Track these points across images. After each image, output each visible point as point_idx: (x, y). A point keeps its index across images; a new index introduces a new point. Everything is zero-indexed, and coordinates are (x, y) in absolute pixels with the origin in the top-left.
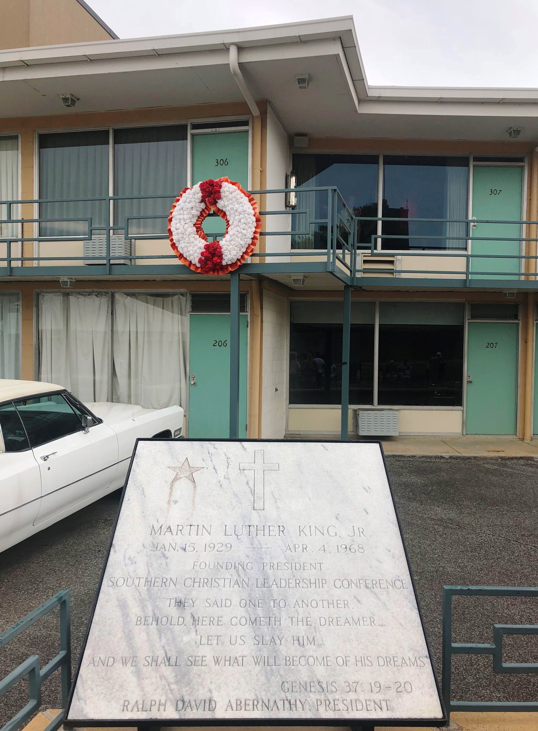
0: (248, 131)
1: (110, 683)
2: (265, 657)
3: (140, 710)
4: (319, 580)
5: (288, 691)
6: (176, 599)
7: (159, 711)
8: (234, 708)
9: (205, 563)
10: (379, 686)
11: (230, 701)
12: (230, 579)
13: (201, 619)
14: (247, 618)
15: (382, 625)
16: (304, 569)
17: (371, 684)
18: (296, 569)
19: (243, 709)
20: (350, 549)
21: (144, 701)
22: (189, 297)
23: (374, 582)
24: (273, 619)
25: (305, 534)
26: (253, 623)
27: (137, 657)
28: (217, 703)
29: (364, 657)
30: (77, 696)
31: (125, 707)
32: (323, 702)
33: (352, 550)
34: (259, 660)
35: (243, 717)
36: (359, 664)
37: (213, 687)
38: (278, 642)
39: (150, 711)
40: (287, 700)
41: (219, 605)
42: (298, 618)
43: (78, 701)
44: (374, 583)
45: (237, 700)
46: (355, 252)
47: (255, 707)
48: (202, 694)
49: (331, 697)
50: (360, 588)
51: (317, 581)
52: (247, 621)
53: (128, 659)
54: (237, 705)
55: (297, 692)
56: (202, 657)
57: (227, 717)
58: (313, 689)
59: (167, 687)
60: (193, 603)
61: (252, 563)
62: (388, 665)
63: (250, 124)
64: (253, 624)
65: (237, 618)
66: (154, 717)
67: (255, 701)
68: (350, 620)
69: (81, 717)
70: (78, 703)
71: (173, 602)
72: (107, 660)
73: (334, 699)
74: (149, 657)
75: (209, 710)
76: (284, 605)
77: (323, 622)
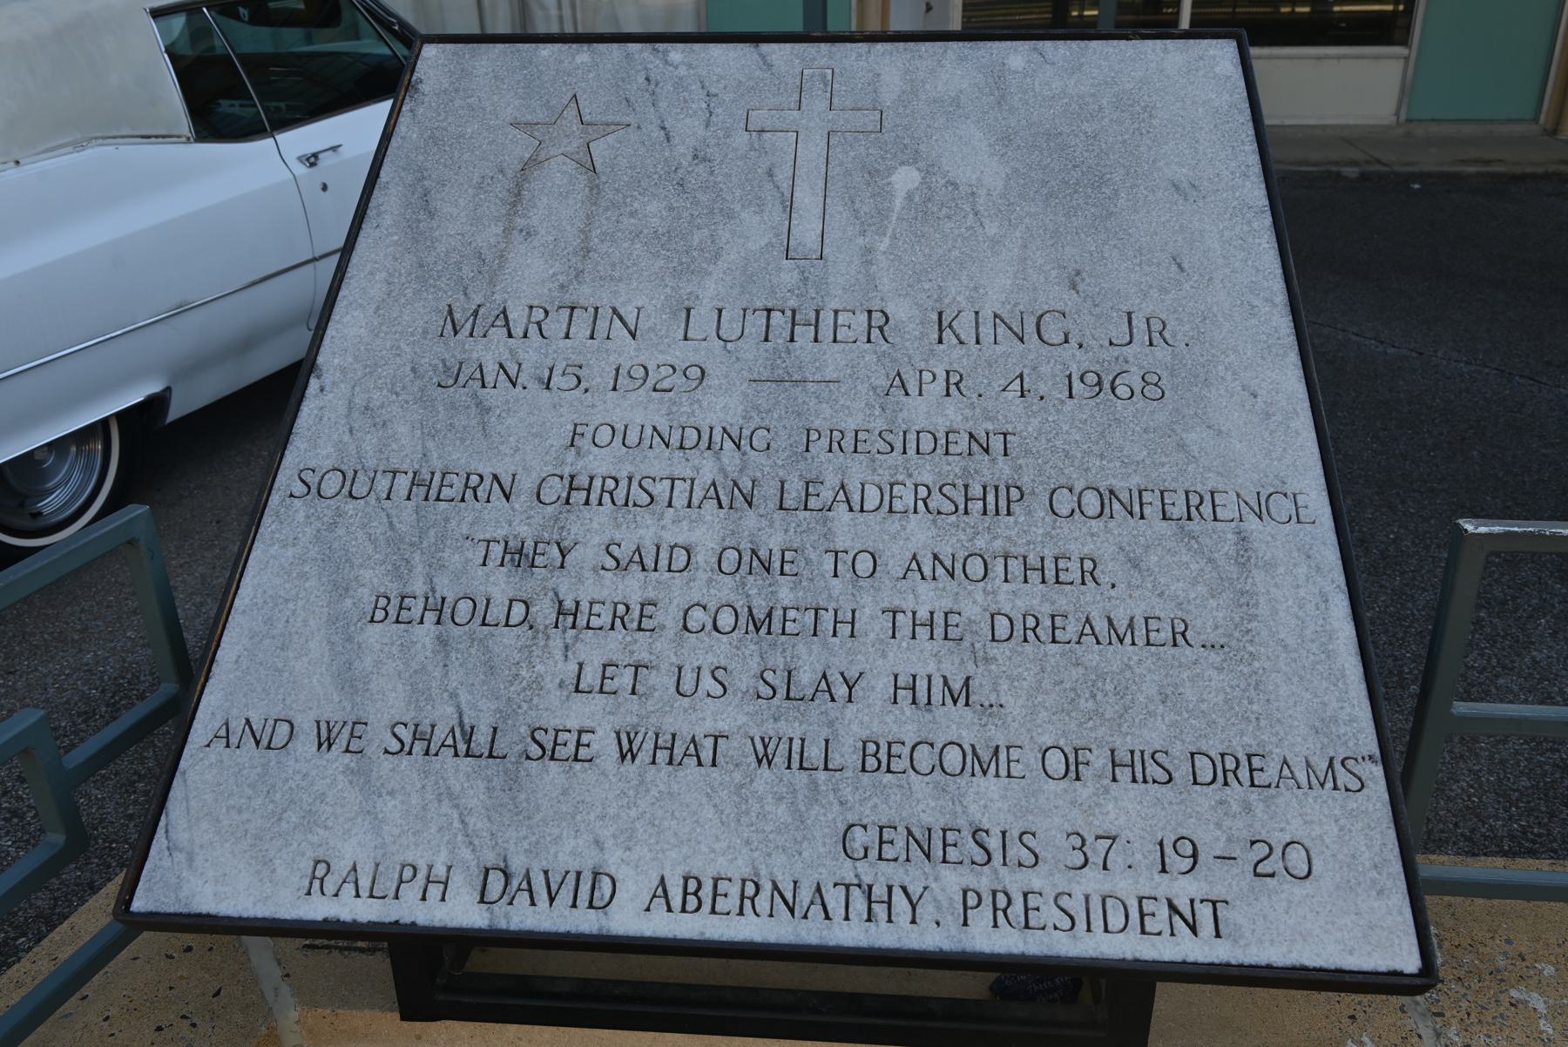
1: (272, 801)
2: (791, 740)
3: (364, 893)
4: (997, 488)
5: (866, 856)
6: (506, 543)
7: (424, 898)
8: (676, 902)
9: (613, 428)
10: (1189, 851)
11: (662, 879)
12: (693, 481)
13: (584, 606)
14: (739, 610)
15: (1213, 646)
16: (947, 453)
17: (1161, 844)
18: (918, 453)
19: (706, 907)
20: (1113, 389)
21: (377, 865)
23: (1194, 500)
24: (827, 618)
25: (957, 336)
26: (759, 625)
27: (366, 724)
28: (617, 884)
29: (1142, 752)
30: (167, 837)
31: (316, 882)
32: (987, 899)
33: (1118, 391)
34: (770, 751)
35: (703, 934)
36: (1124, 774)
37: (605, 833)
38: (841, 691)
39: (397, 897)
40: (859, 886)
41: (649, 563)
42: (914, 613)
43: (167, 853)
44: (1191, 503)
45: (686, 879)
47: (747, 903)
48: (570, 853)
49: (1015, 882)
50: (1142, 517)
52: (740, 617)
53: (336, 730)
54: (685, 893)
55: (896, 860)
56: (580, 732)
57: (648, 933)
58: (952, 854)
59: (457, 824)
60: (564, 557)
61: (768, 430)
62: (1229, 780)
64: (757, 632)
65: (705, 608)
66: (407, 920)
67: (748, 883)
68: (1101, 626)
69: (170, 906)
70: (167, 863)
71: (497, 550)
72: (269, 729)
73: (1026, 890)
74: (406, 725)
75: (591, 906)
76: (871, 570)
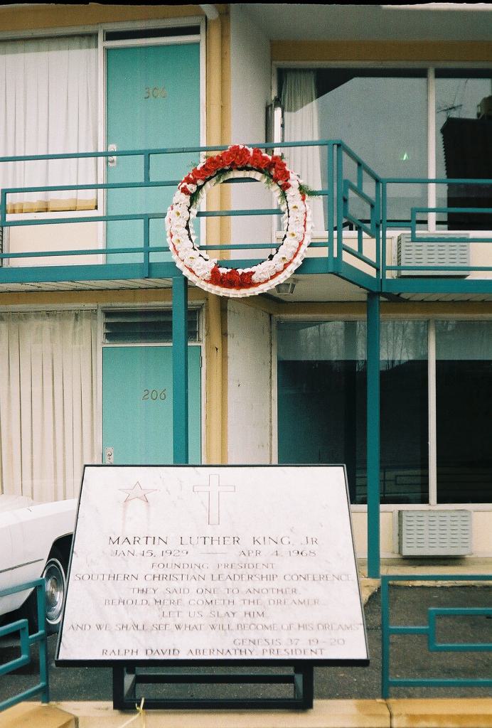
0: (198, 44)
22: (101, 320)
36: (302, 629)
46: (384, 234)
49: (273, 647)
51: (268, 577)
63: (202, 30)
68: (297, 602)
77: (272, 602)
